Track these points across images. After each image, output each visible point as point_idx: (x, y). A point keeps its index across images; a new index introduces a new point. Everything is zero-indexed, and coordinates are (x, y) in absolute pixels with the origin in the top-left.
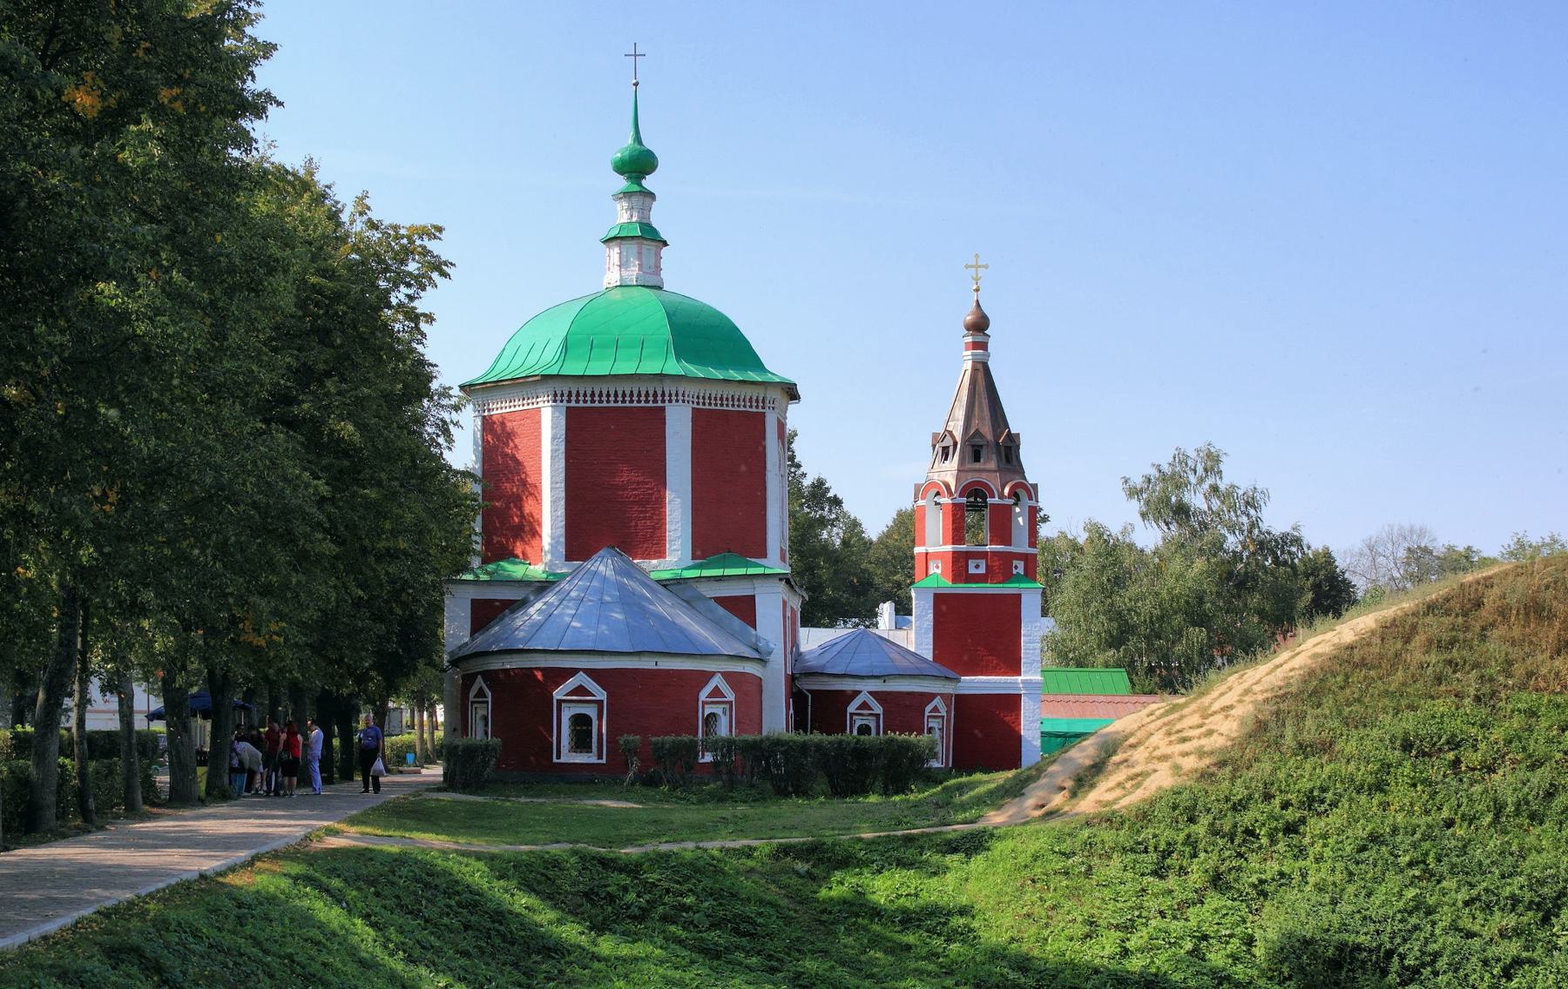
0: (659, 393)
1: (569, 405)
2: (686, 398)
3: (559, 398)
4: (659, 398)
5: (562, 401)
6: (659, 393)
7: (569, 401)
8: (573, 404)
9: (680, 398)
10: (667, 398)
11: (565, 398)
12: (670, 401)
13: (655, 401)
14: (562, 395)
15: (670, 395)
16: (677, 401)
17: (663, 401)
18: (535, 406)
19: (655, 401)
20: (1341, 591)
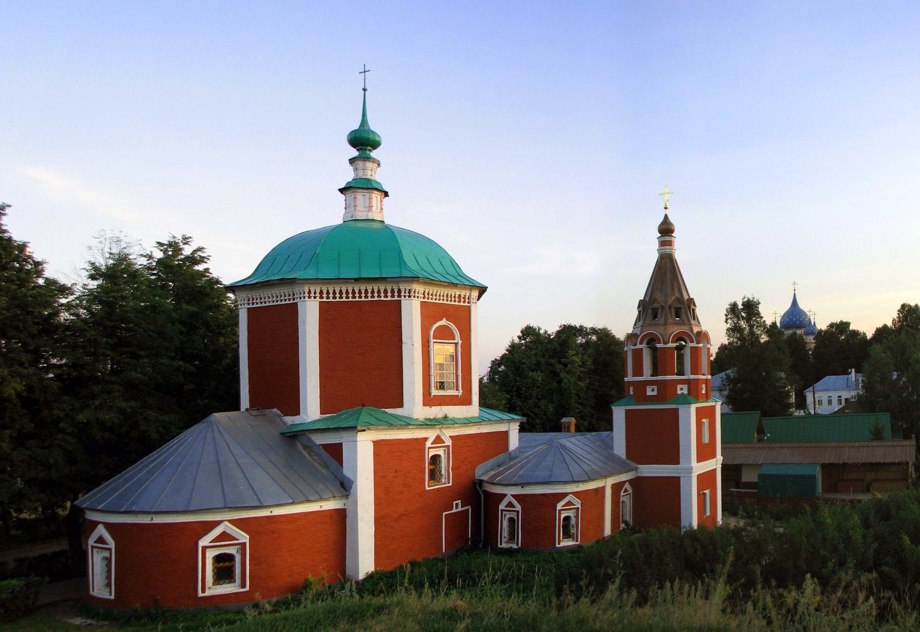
2: (417, 295)
4: (396, 294)
9: (412, 294)
10: (403, 294)
12: (405, 296)
13: (393, 296)
16: (410, 296)
19: (393, 296)
20: (788, 398)
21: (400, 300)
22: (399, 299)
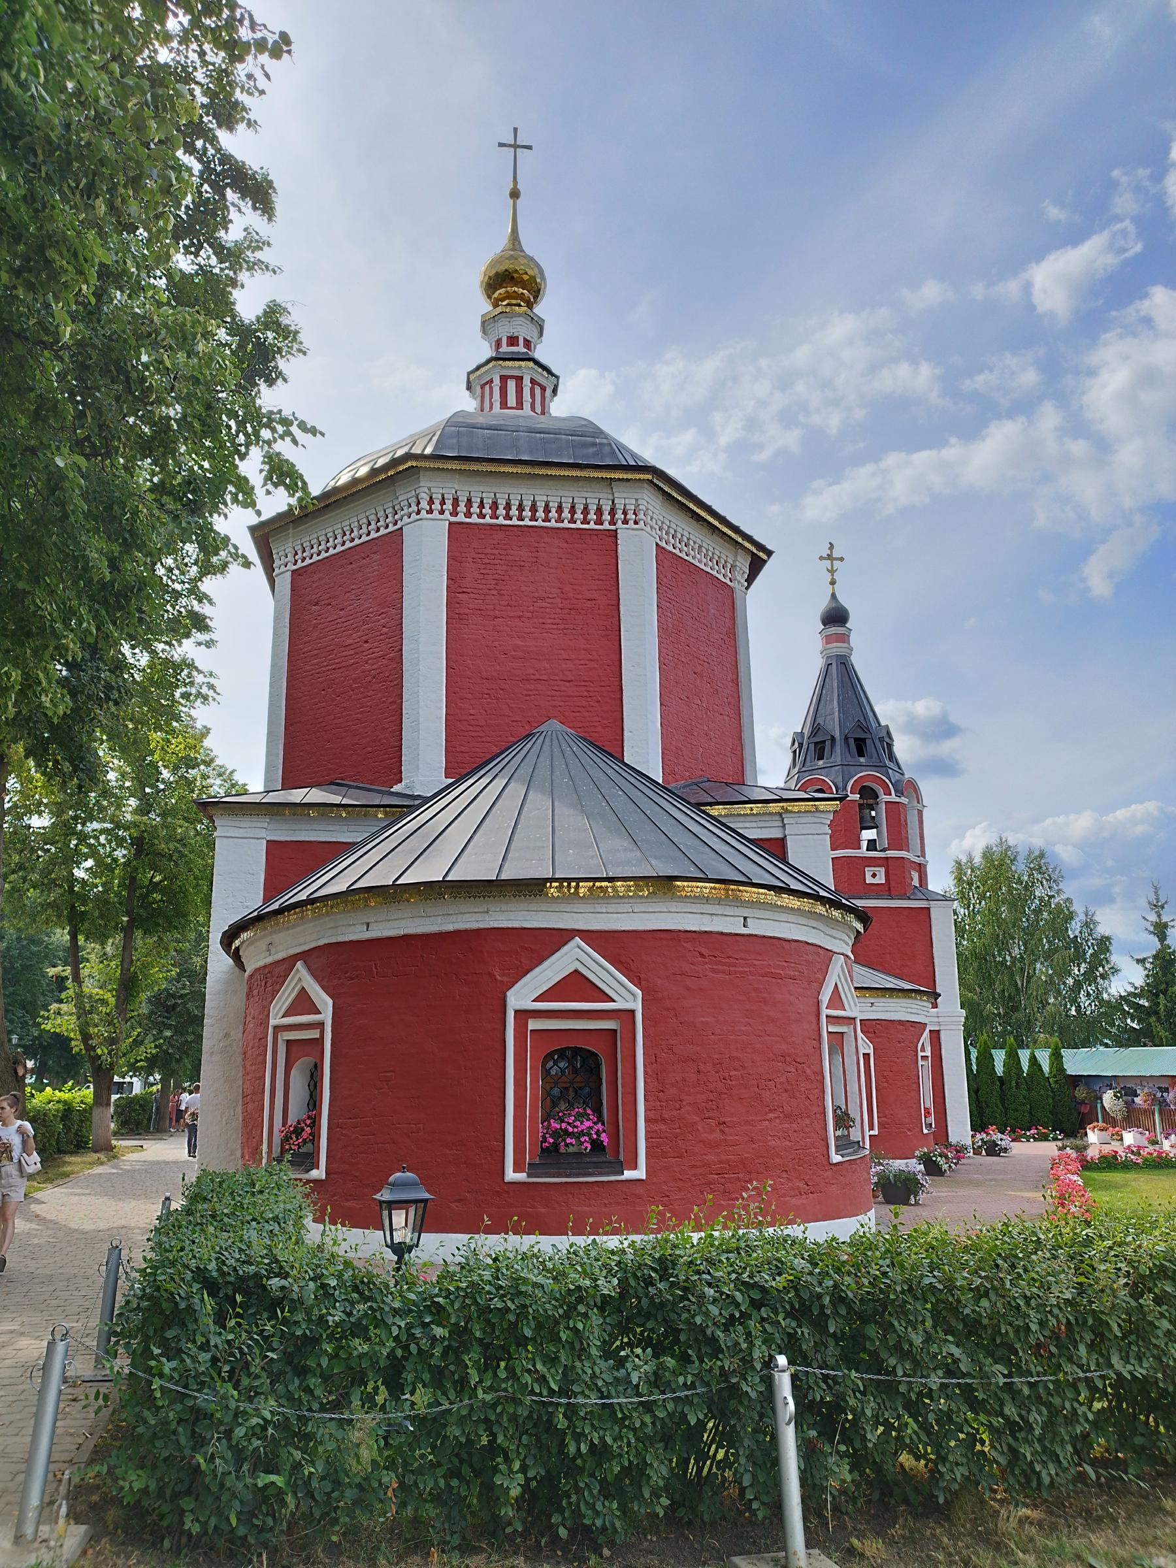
0: (606, 509)
1: (453, 519)
3: (437, 506)
4: (606, 517)
5: (442, 512)
6: (606, 509)
7: (455, 513)
8: (461, 518)
10: (619, 515)
11: (448, 506)
12: (625, 522)
13: (599, 522)
14: (443, 503)
15: (625, 513)
17: (612, 523)
18: (391, 528)
19: (599, 522)
21: (616, 531)
22: (613, 528)
